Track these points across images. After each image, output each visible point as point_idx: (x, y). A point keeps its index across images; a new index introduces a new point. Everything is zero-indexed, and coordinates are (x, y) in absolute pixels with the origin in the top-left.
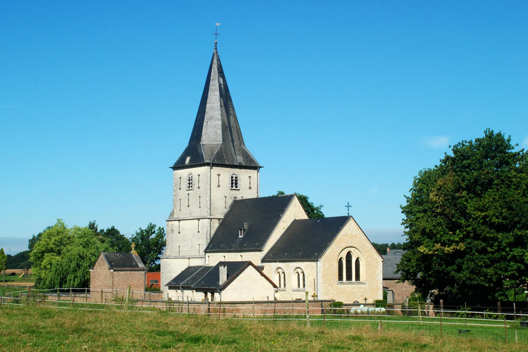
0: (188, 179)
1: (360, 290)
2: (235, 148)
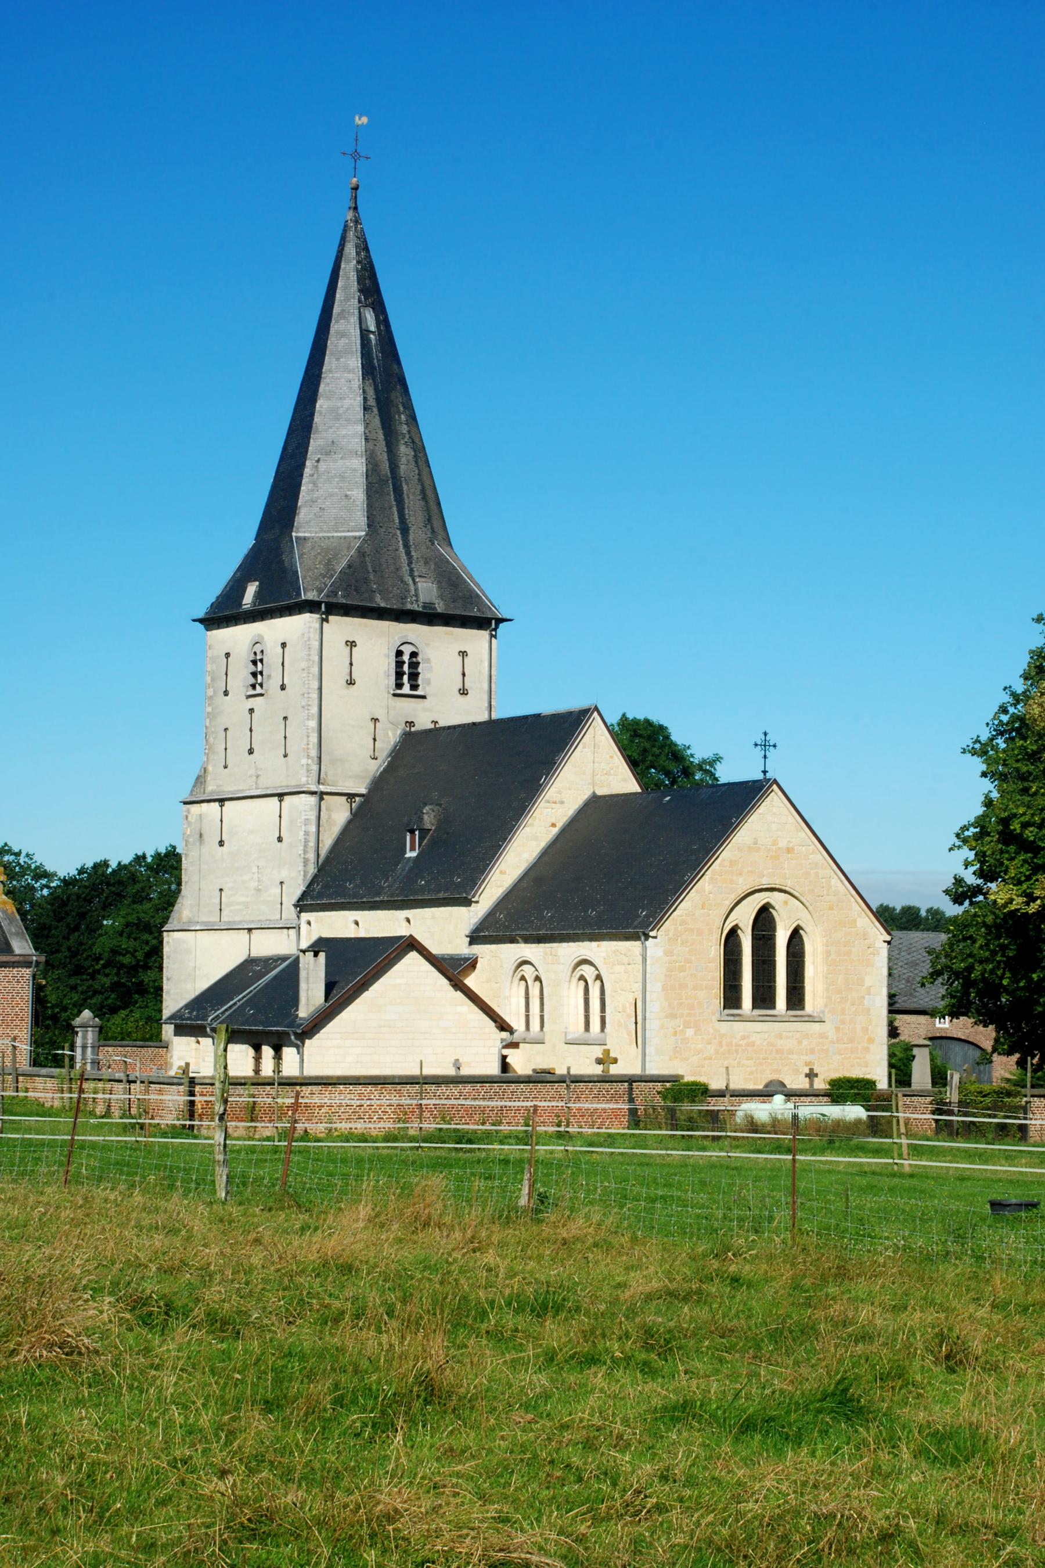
0: (252, 657)
2: (413, 553)
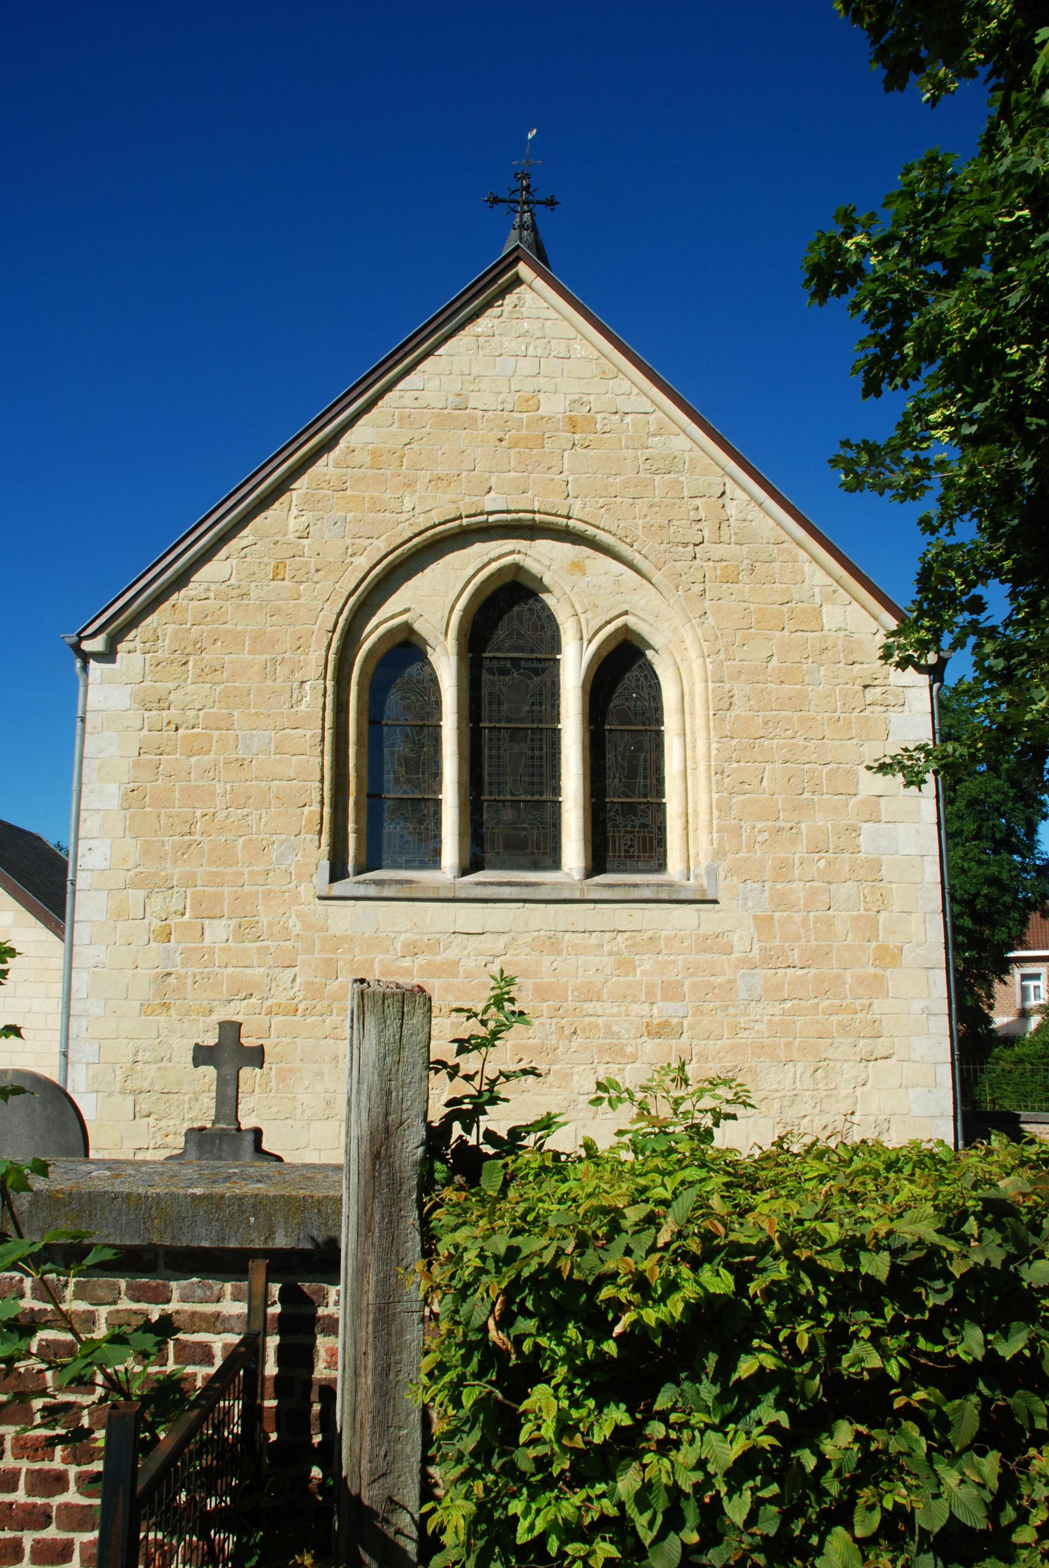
1: (646, 964)
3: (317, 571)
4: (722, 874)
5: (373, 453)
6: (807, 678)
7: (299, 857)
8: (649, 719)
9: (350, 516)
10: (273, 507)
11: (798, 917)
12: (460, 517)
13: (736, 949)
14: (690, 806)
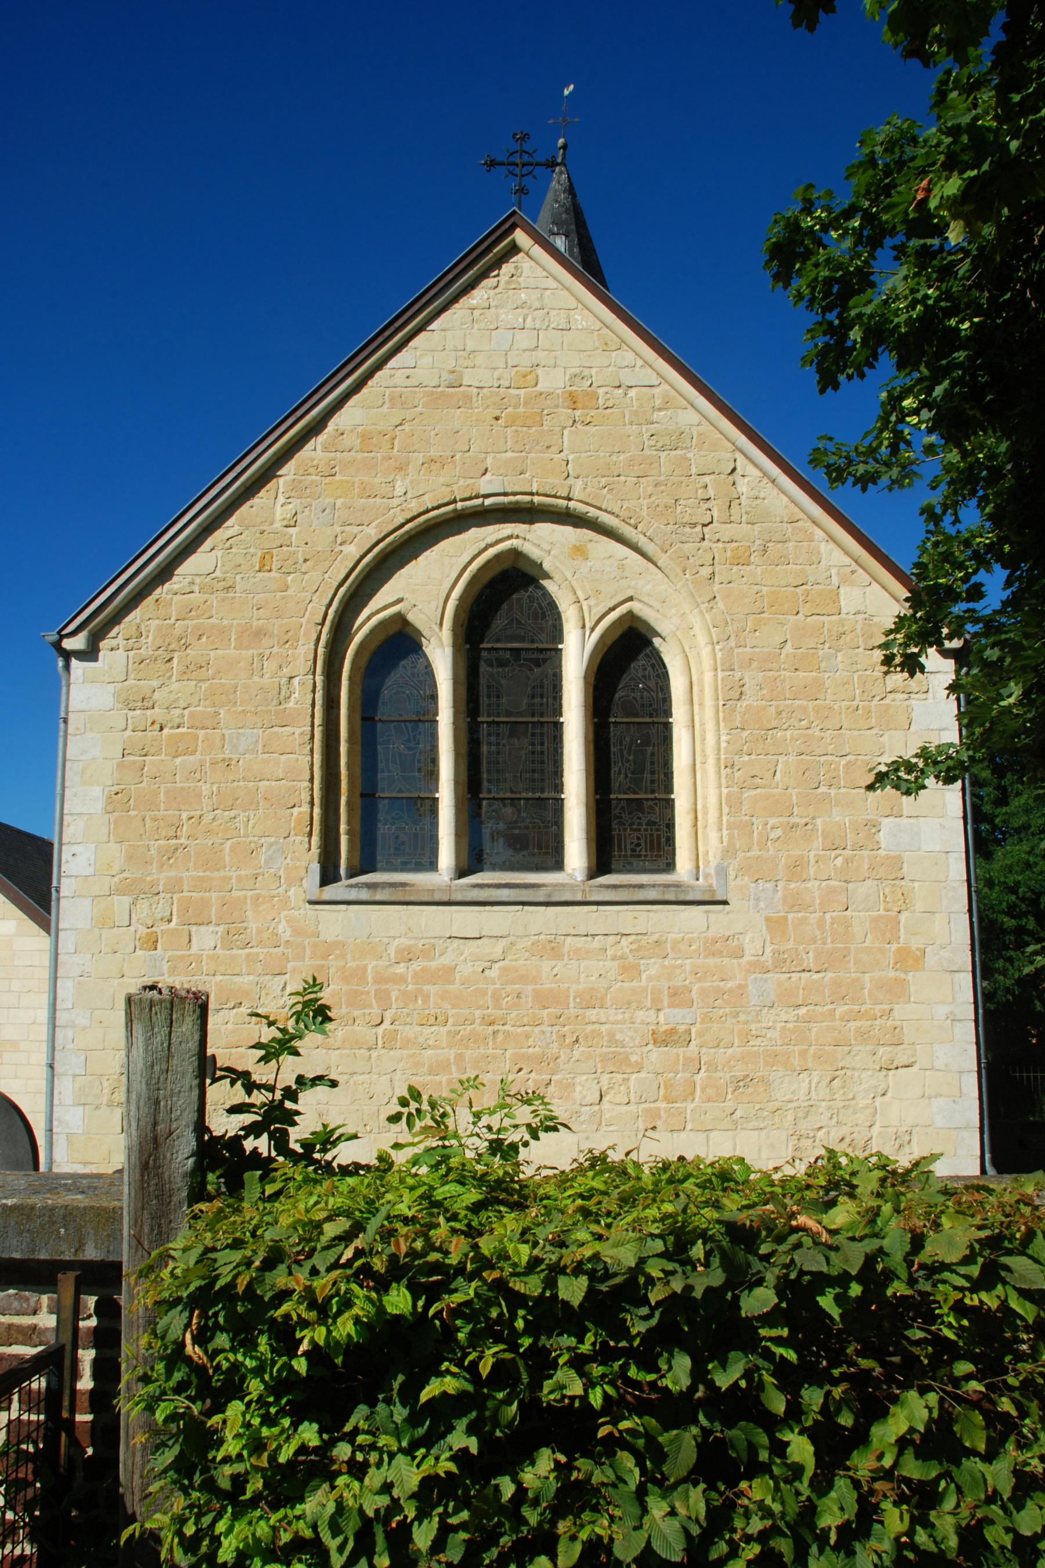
1: (652, 968)
3: (305, 561)
4: (732, 873)
5: (363, 436)
6: (823, 665)
7: (288, 861)
8: (656, 710)
9: (339, 502)
10: (260, 495)
11: (813, 918)
12: (455, 501)
13: (747, 952)
14: (699, 802)
